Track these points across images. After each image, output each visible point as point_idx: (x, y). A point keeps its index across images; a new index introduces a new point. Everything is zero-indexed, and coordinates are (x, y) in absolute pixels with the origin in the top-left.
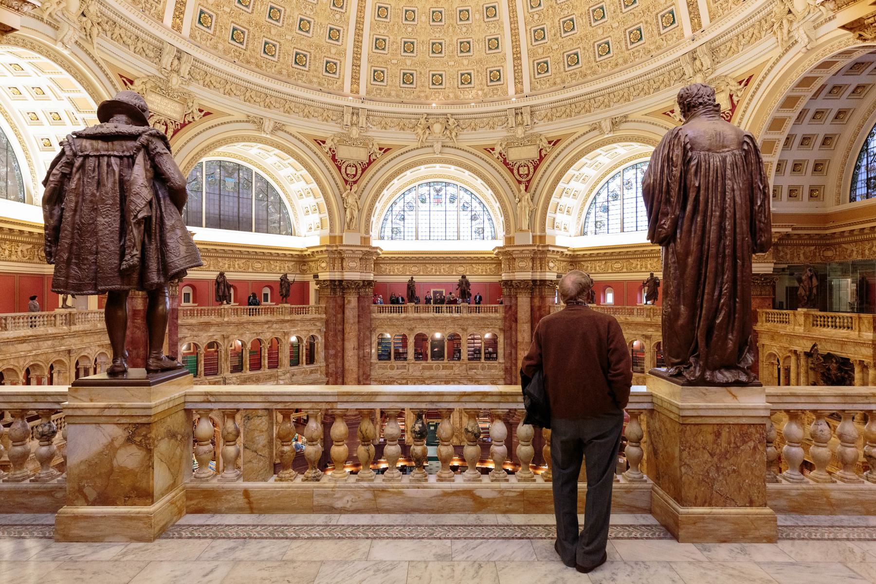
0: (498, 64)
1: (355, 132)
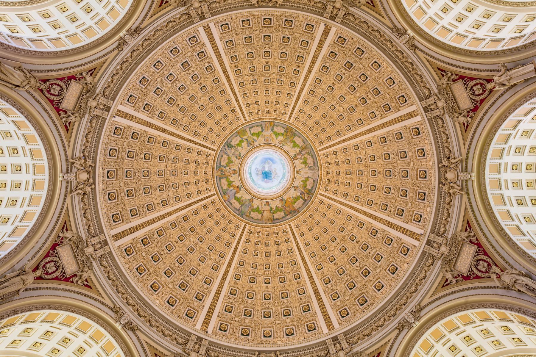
0: (311, 318)
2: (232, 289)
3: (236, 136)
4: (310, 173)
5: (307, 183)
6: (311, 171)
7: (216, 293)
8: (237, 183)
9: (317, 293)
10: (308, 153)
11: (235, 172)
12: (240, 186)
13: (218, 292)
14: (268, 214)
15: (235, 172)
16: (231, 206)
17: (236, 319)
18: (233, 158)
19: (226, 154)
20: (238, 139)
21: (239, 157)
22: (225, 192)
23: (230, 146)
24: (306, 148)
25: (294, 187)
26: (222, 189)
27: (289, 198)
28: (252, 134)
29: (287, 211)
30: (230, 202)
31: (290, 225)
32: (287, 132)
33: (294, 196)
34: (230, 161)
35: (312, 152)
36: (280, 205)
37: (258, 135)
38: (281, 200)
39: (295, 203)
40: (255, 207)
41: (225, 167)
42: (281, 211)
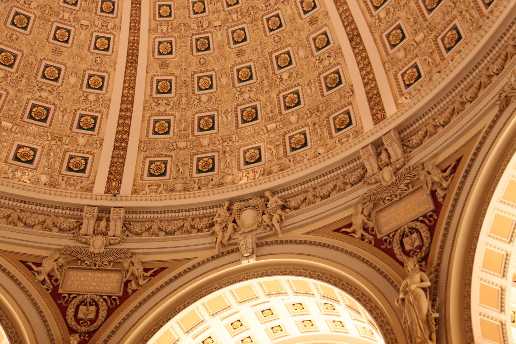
1: (98, 244)
2: (158, 81)
7: (123, 102)
9: (354, 37)
13: (127, 100)
17: (182, 144)
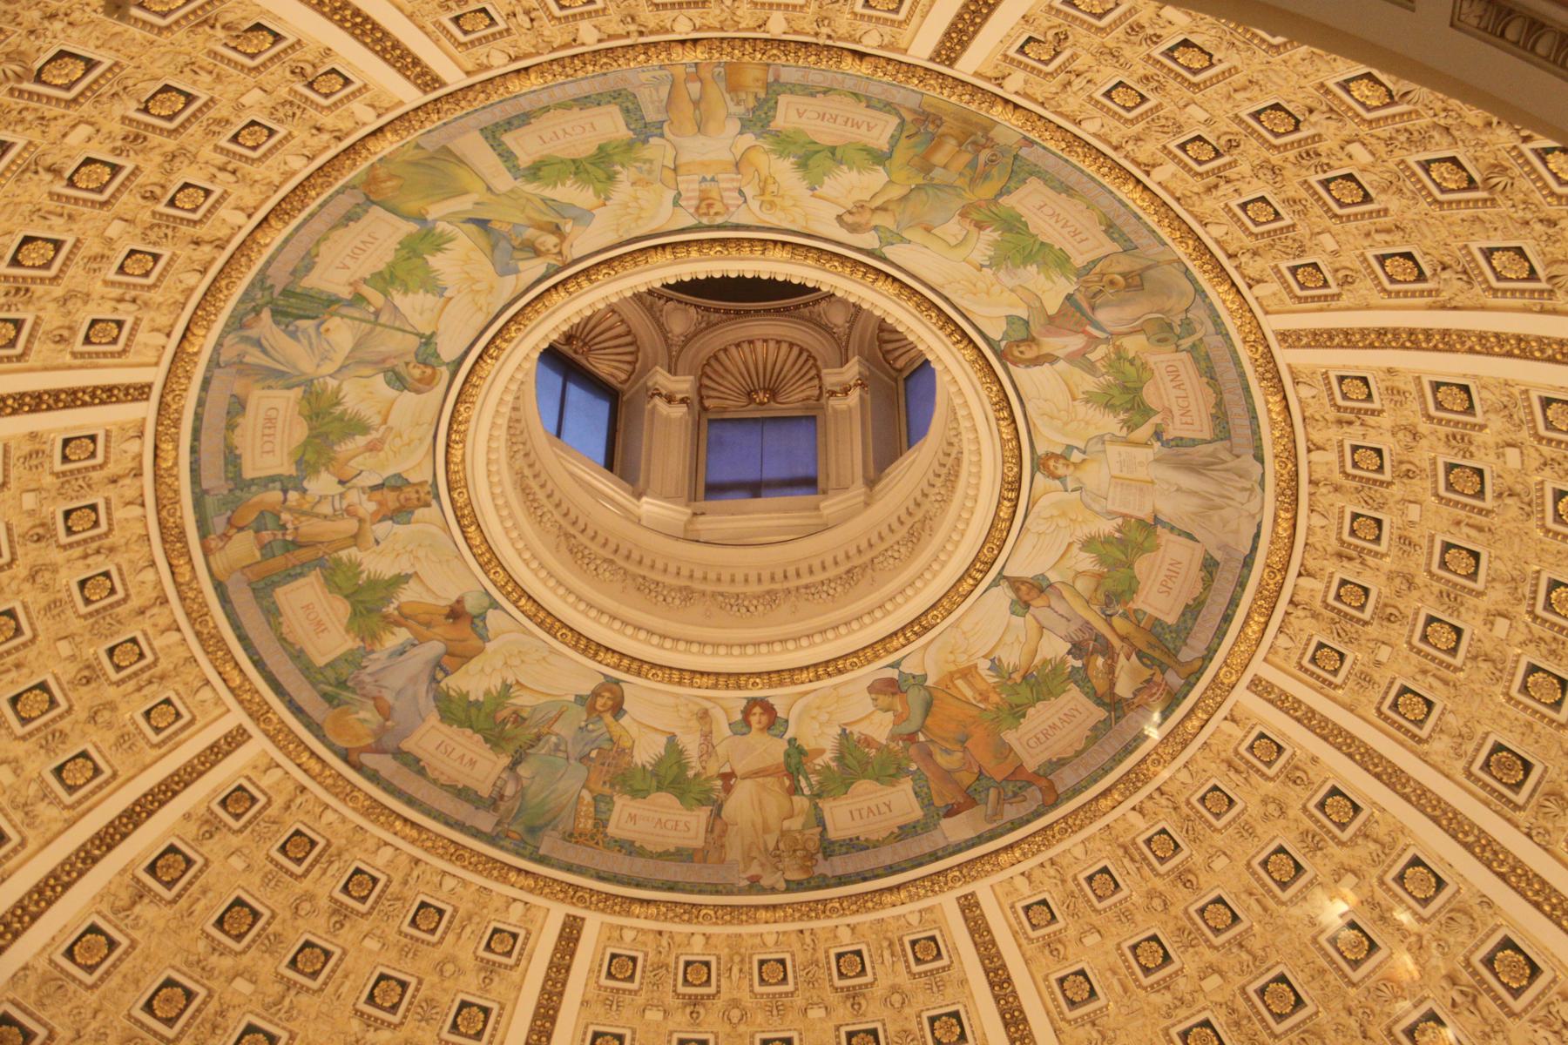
3: (349, 218)
4: (1170, 494)
5: (1141, 566)
6: (1188, 481)
8: (446, 579)
10: (1165, 332)
11: (399, 498)
12: (471, 606)
14: (775, 802)
15: (399, 498)
16: (414, 786)
18: (363, 395)
19: (276, 376)
20: (383, 234)
21: (418, 367)
22: (338, 685)
23: (294, 305)
24: (1135, 282)
25: (1015, 583)
26: (306, 668)
27: (968, 673)
28: (535, 172)
29: (947, 775)
30: (400, 755)
31: (969, 906)
32: (935, 142)
33: (1012, 657)
34: (327, 426)
35: (1205, 329)
36: (879, 727)
37: (598, 167)
38: (889, 688)
39: (1017, 713)
40: (647, 751)
41: (286, 484)
42: (888, 770)
